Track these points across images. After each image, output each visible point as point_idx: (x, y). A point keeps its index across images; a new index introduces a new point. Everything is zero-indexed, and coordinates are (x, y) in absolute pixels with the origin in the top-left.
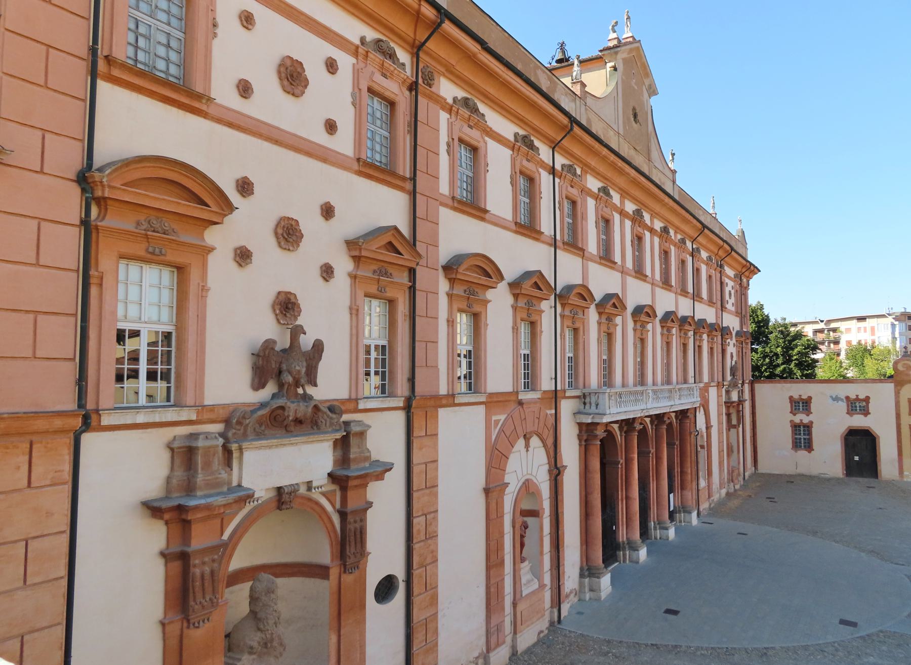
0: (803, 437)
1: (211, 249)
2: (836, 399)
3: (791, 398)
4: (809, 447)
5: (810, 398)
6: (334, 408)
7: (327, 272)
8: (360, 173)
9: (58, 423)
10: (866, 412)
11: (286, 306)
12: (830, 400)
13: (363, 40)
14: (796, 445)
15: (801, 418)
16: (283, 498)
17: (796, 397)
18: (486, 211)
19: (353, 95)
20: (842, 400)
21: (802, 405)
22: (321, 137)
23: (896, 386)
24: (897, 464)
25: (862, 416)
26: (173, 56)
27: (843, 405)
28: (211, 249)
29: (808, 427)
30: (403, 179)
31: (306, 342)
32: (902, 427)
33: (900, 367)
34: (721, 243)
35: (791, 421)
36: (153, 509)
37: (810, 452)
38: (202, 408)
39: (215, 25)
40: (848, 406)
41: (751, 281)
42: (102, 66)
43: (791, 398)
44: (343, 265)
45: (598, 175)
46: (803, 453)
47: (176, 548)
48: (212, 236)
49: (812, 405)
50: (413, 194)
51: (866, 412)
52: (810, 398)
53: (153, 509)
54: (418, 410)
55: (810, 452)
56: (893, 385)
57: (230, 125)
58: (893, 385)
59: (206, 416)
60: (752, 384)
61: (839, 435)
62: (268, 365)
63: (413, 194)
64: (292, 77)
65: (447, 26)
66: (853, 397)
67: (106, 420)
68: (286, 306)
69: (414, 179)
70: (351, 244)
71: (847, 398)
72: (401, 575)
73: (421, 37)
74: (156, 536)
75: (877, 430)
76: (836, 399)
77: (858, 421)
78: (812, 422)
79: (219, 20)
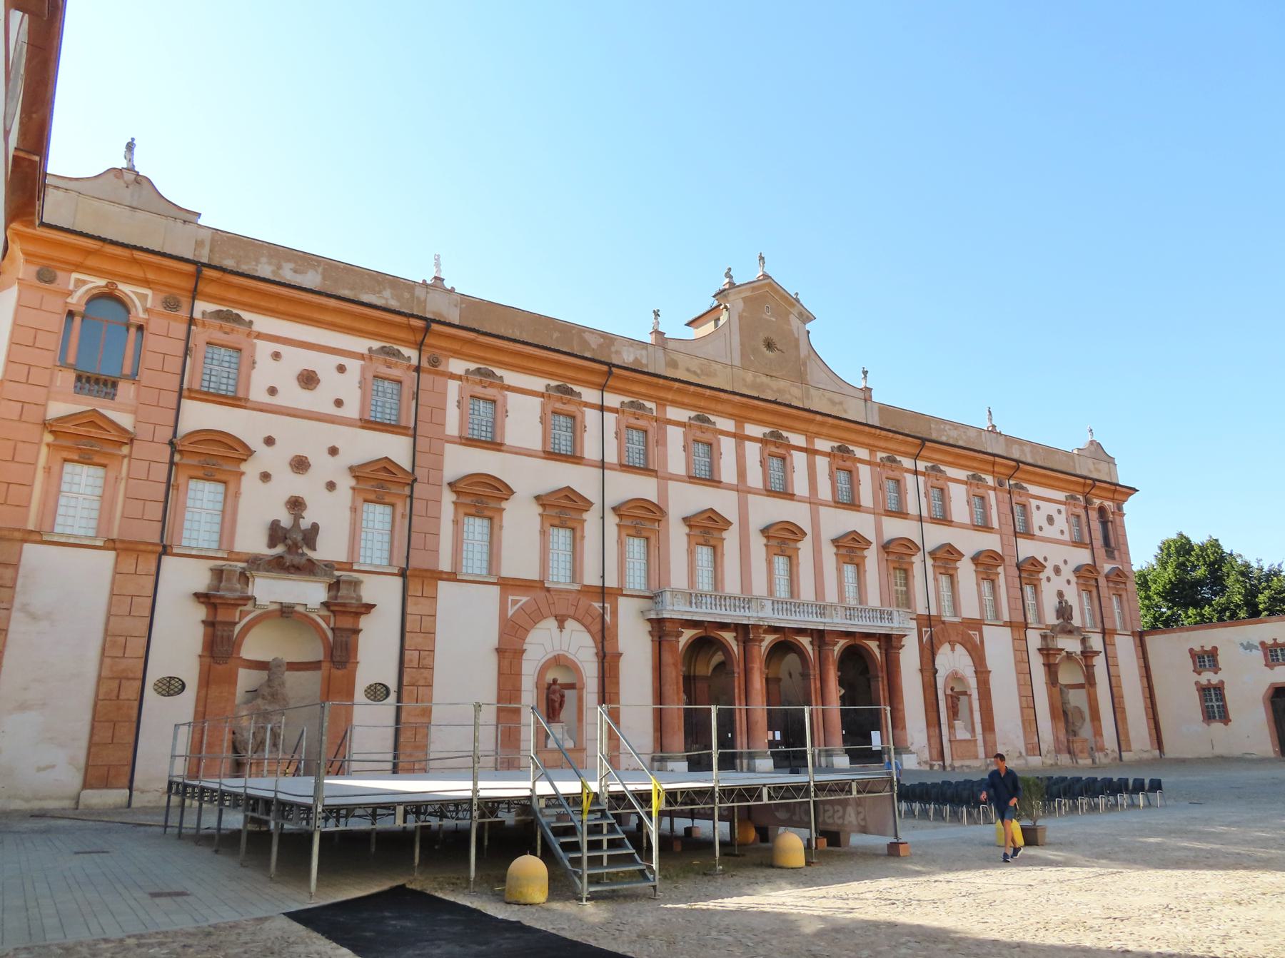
0: (1214, 704)
1: (243, 474)
2: (1248, 647)
3: (1191, 651)
4: (1225, 718)
5: (1215, 649)
6: (330, 566)
7: (331, 486)
8: (363, 427)
9: (150, 548)
11: (296, 505)
12: (1241, 649)
13: (370, 350)
14: (1209, 716)
15: (1208, 677)
16: (286, 612)
17: (1197, 649)
18: (501, 444)
19: (360, 382)
20: (1256, 648)
21: (1205, 659)
22: (332, 410)
26: (231, 382)
27: (1258, 655)
28: (243, 474)
29: (1219, 689)
30: (406, 428)
31: (305, 524)
34: (991, 458)
35: (1197, 683)
36: (200, 597)
37: (1226, 724)
38: (231, 552)
39: (254, 363)
40: (1265, 655)
41: (1126, 507)
42: (185, 393)
43: (1191, 651)
44: (346, 483)
45: (674, 403)
46: (1217, 726)
47: (210, 619)
48: (244, 467)
50: (414, 437)
52: (1215, 649)
53: (200, 597)
54: (417, 577)
55: (1226, 724)
57: (261, 410)
59: (234, 557)
60: (1140, 636)
62: (276, 534)
63: (414, 437)
64: (308, 380)
65: (435, 327)
67: (175, 551)
68: (296, 505)
69: (415, 428)
70: (351, 469)
71: (1263, 644)
72: (393, 686)
73: (419, 338)
74: (201, 612)
76: (1248, 647)
78: (1222, 682)
79: (257, 359)
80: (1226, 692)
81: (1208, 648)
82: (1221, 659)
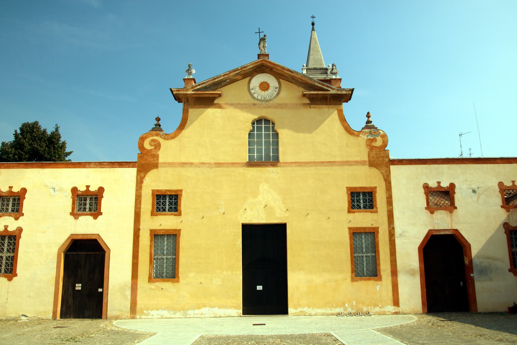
10: (96, 212)
23: (139, 172)
24: (128, 293)
25: (91, 218)
32: (141, 233)
33: (147, 145)
37: (10, 279)
49: (26, 203)
51: (96, 212)
52: (24, 191)
55: (10, 279)
56: (135, 169)
58: (135, 169)
61: (55, 250)
66: (82, 188)
75: (109, 240)
77: (86, 226)
78: (20, 230)
80: (21, 241)
81: (16, 190)
82: (27, 205)
